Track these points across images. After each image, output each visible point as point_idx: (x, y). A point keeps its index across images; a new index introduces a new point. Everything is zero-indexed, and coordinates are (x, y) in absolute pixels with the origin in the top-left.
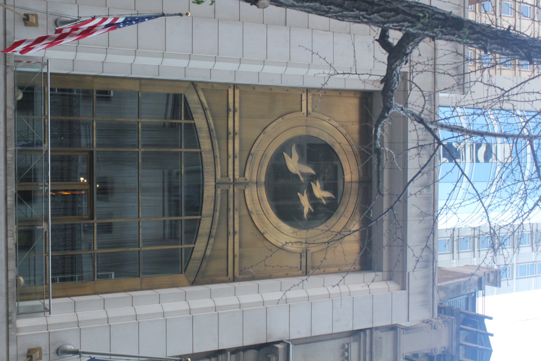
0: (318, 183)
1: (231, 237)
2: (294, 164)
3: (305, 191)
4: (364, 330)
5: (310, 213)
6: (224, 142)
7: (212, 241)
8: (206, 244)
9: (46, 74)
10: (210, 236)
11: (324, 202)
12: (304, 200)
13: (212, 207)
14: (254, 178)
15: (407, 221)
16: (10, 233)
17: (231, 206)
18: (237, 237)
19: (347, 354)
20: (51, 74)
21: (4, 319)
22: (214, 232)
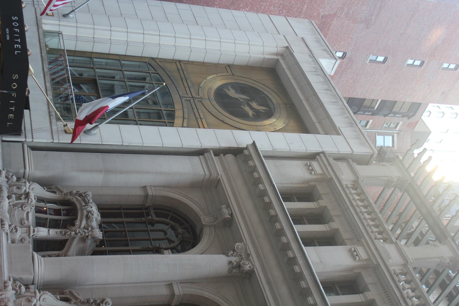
0: (253, 102)
1: (199, 120)
2: (232, 93)
3: (246, 105)
4: (318, 154)
5: (253, 115)
6: (180, 82)
7: (186, 120)
8: (182, 121)
9: (63, 50)
10: (184, 118)
11: (263, 111)
12: (247, 109)
13: (181, 106)
14: (207, 97)
15: (323, 104)
16: (47, 81)
17: (194, 107)
18: (203, 120)
19: (311, 168)
20: (67, 50)
21: (47, 114)
22: (186, 116)
